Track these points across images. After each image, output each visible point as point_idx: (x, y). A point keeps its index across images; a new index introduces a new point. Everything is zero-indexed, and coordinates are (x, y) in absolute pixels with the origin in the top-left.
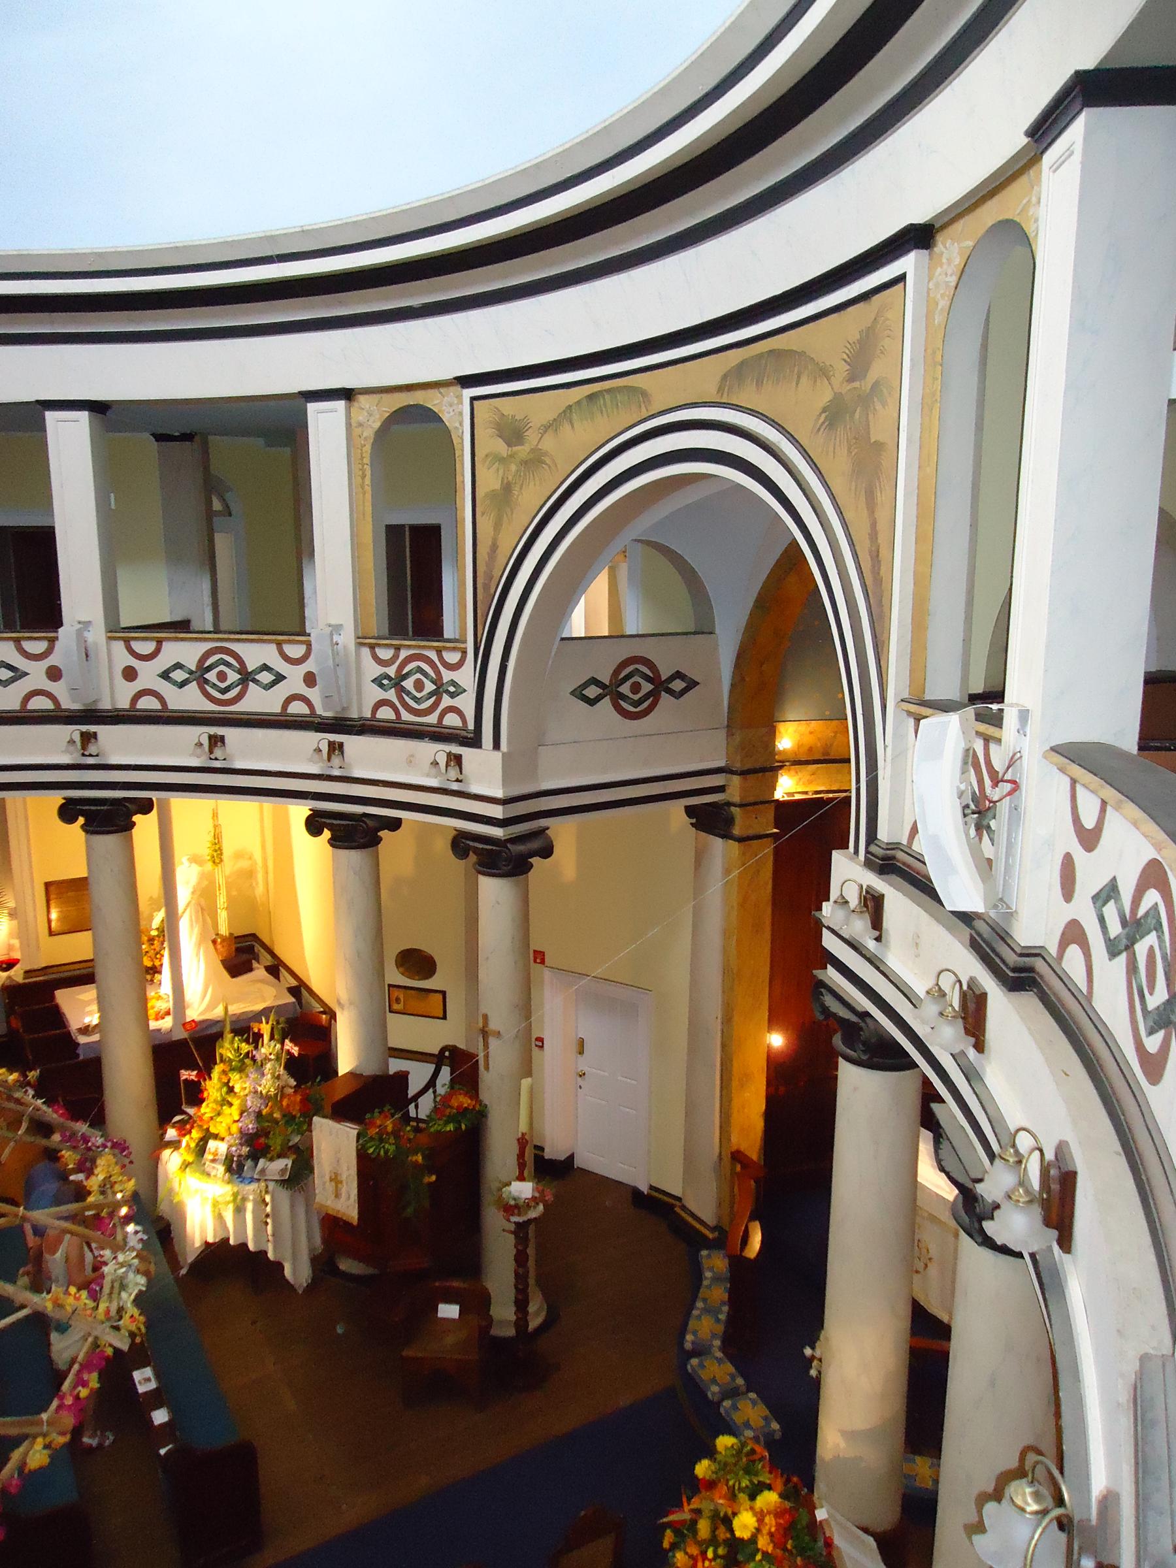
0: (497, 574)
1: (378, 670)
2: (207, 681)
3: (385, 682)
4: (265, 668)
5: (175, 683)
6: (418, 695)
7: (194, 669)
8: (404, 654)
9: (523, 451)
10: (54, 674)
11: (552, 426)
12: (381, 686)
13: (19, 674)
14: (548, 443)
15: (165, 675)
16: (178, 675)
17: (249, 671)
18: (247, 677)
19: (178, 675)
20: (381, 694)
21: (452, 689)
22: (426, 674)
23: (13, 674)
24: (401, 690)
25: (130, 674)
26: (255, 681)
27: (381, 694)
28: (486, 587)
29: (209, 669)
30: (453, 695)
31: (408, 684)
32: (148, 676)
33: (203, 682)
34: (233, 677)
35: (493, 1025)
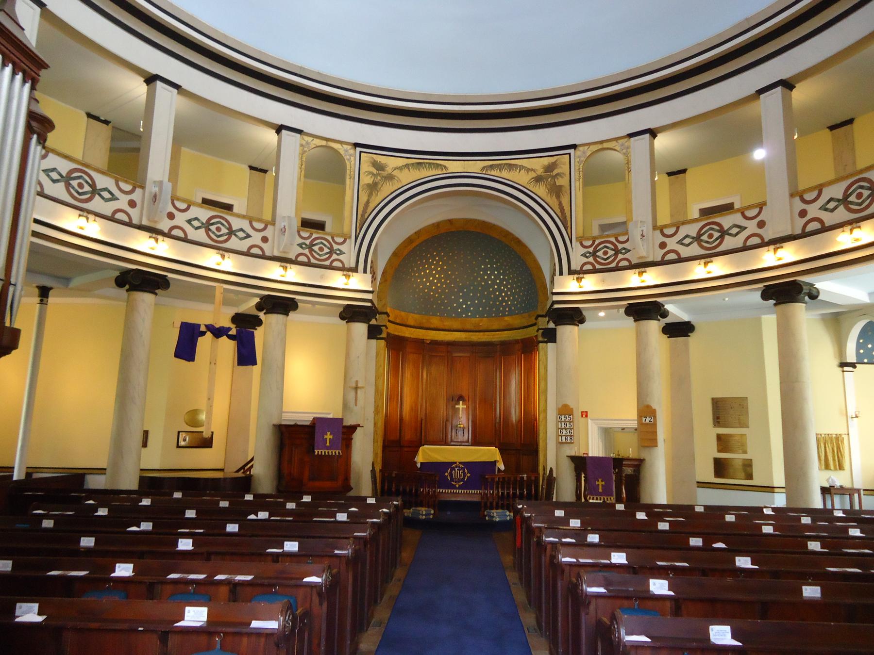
0: (369, 211)
1: (301, 241)
2: (210, 230)
3: (304, 246)
4: (241, 230)
5: (193, 226)
6: (321, 253)
7: (204, 222)
8: (314, 236)
9: (384, 173)
10: (132, 204)
11: (400, 168)
12: (302, 247)
13: (114, 197)
14: (396, 173)
15: (189, 222)
16: (196, 223)
17: (234, 229)
18: (231, 232)
19: (196, 223)
20: (300, 251)
21: (338, 252)
22: (325, 245)
23: (111, 197)
24: (311, 250)
25: (171, 216)
26: (235, 235)
27: (300, 251)
28: (363, 215)
29: (213, 224)
30: (338, 255)
31: (316, 248)
32: (180, 219)
33: (208, 230)
34: (224, 231)
35: (360, 385)
